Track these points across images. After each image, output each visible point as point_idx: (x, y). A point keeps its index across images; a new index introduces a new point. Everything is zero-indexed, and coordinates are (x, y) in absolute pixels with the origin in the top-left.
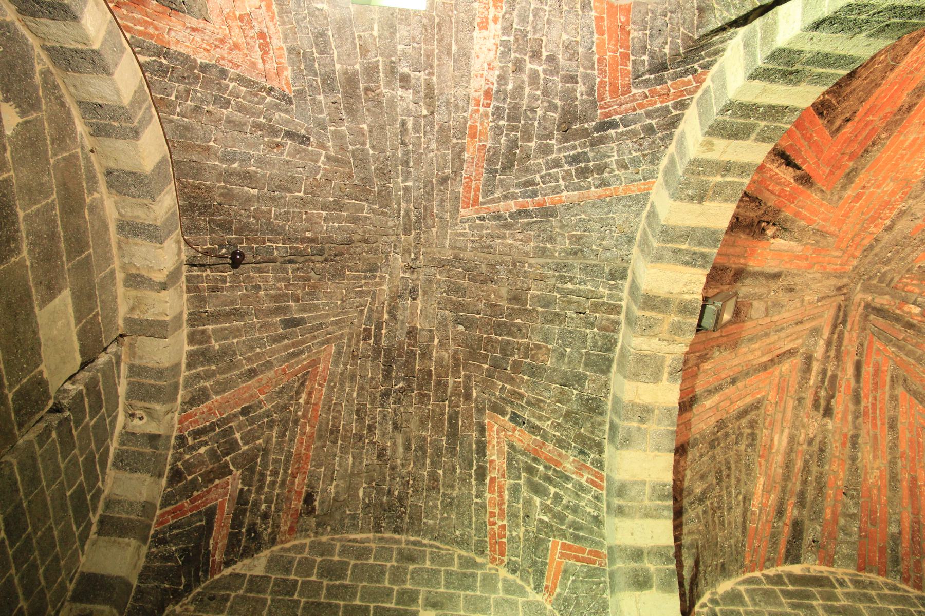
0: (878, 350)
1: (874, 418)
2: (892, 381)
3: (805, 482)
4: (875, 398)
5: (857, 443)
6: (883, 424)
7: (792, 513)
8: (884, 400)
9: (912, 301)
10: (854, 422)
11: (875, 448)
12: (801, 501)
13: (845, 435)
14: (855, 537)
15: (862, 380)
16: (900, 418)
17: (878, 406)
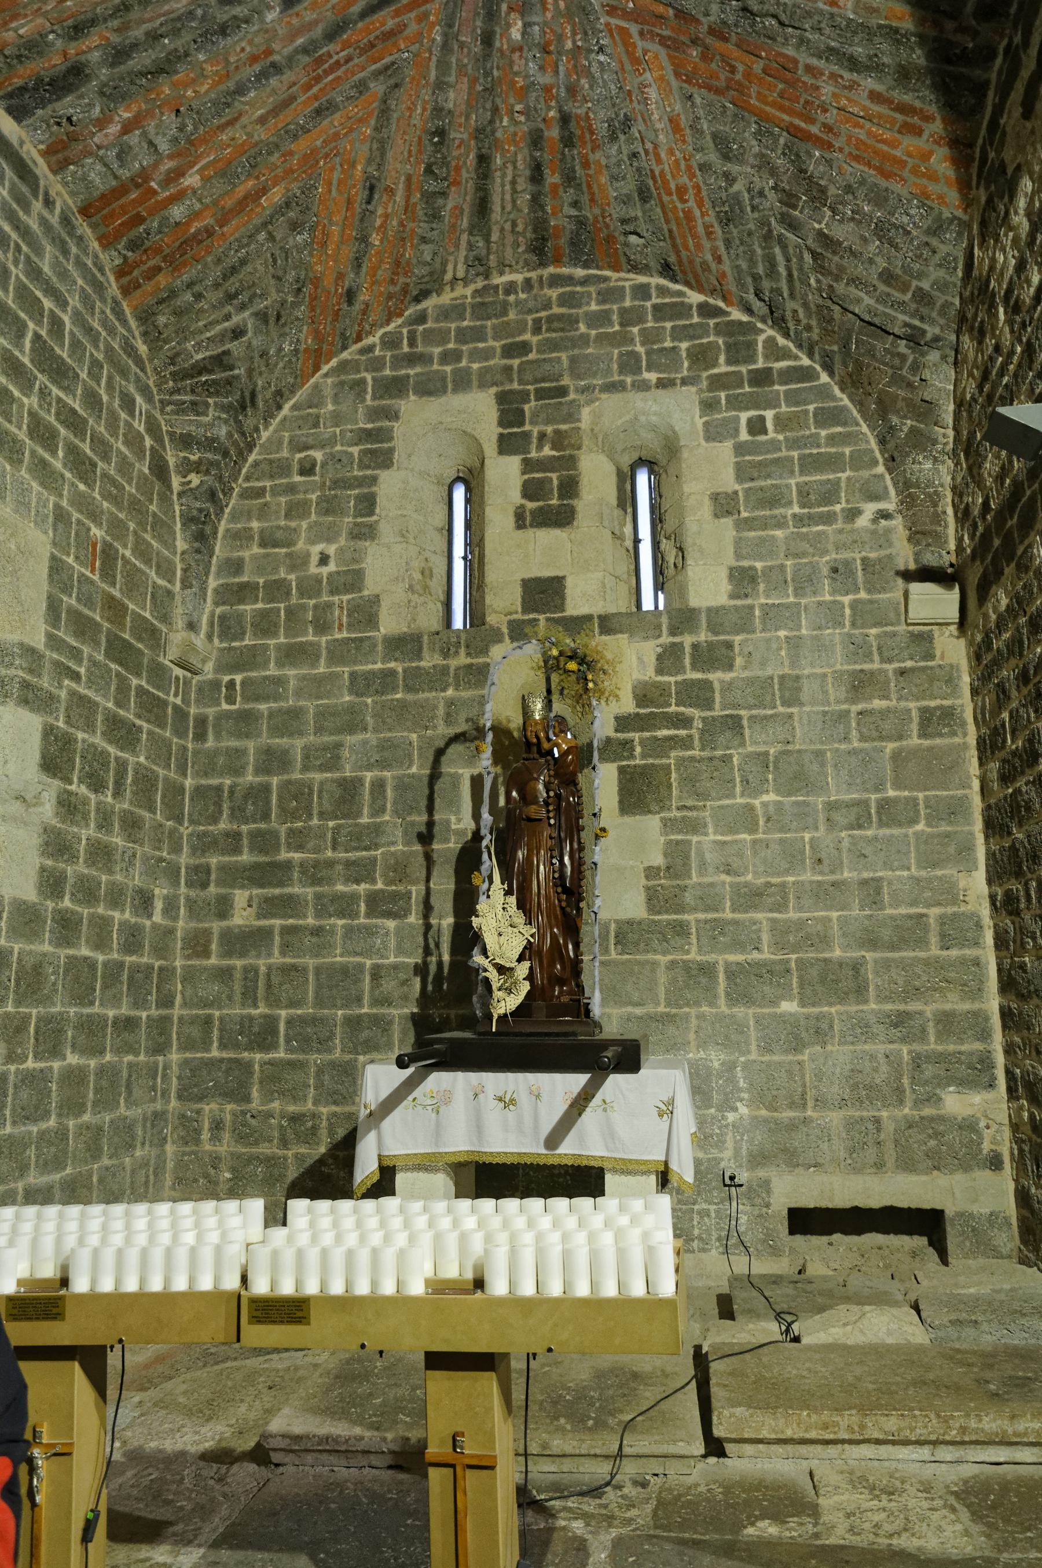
0: (426, 15)
1: (318, 79)
2: (387, 68)
3: (154, 37)
4: (349, 59)
5: (267, 79)
6: (316, 97)
7: (90, 49)
8: (353, 74)
9: (528, 19)
10: (296, 51)
11: (275, 111)
12: (119, 54)
13: (268, 52)
14: (125, 174)
15: (367, 20)
16: (337, 115)
17: (339, 73)
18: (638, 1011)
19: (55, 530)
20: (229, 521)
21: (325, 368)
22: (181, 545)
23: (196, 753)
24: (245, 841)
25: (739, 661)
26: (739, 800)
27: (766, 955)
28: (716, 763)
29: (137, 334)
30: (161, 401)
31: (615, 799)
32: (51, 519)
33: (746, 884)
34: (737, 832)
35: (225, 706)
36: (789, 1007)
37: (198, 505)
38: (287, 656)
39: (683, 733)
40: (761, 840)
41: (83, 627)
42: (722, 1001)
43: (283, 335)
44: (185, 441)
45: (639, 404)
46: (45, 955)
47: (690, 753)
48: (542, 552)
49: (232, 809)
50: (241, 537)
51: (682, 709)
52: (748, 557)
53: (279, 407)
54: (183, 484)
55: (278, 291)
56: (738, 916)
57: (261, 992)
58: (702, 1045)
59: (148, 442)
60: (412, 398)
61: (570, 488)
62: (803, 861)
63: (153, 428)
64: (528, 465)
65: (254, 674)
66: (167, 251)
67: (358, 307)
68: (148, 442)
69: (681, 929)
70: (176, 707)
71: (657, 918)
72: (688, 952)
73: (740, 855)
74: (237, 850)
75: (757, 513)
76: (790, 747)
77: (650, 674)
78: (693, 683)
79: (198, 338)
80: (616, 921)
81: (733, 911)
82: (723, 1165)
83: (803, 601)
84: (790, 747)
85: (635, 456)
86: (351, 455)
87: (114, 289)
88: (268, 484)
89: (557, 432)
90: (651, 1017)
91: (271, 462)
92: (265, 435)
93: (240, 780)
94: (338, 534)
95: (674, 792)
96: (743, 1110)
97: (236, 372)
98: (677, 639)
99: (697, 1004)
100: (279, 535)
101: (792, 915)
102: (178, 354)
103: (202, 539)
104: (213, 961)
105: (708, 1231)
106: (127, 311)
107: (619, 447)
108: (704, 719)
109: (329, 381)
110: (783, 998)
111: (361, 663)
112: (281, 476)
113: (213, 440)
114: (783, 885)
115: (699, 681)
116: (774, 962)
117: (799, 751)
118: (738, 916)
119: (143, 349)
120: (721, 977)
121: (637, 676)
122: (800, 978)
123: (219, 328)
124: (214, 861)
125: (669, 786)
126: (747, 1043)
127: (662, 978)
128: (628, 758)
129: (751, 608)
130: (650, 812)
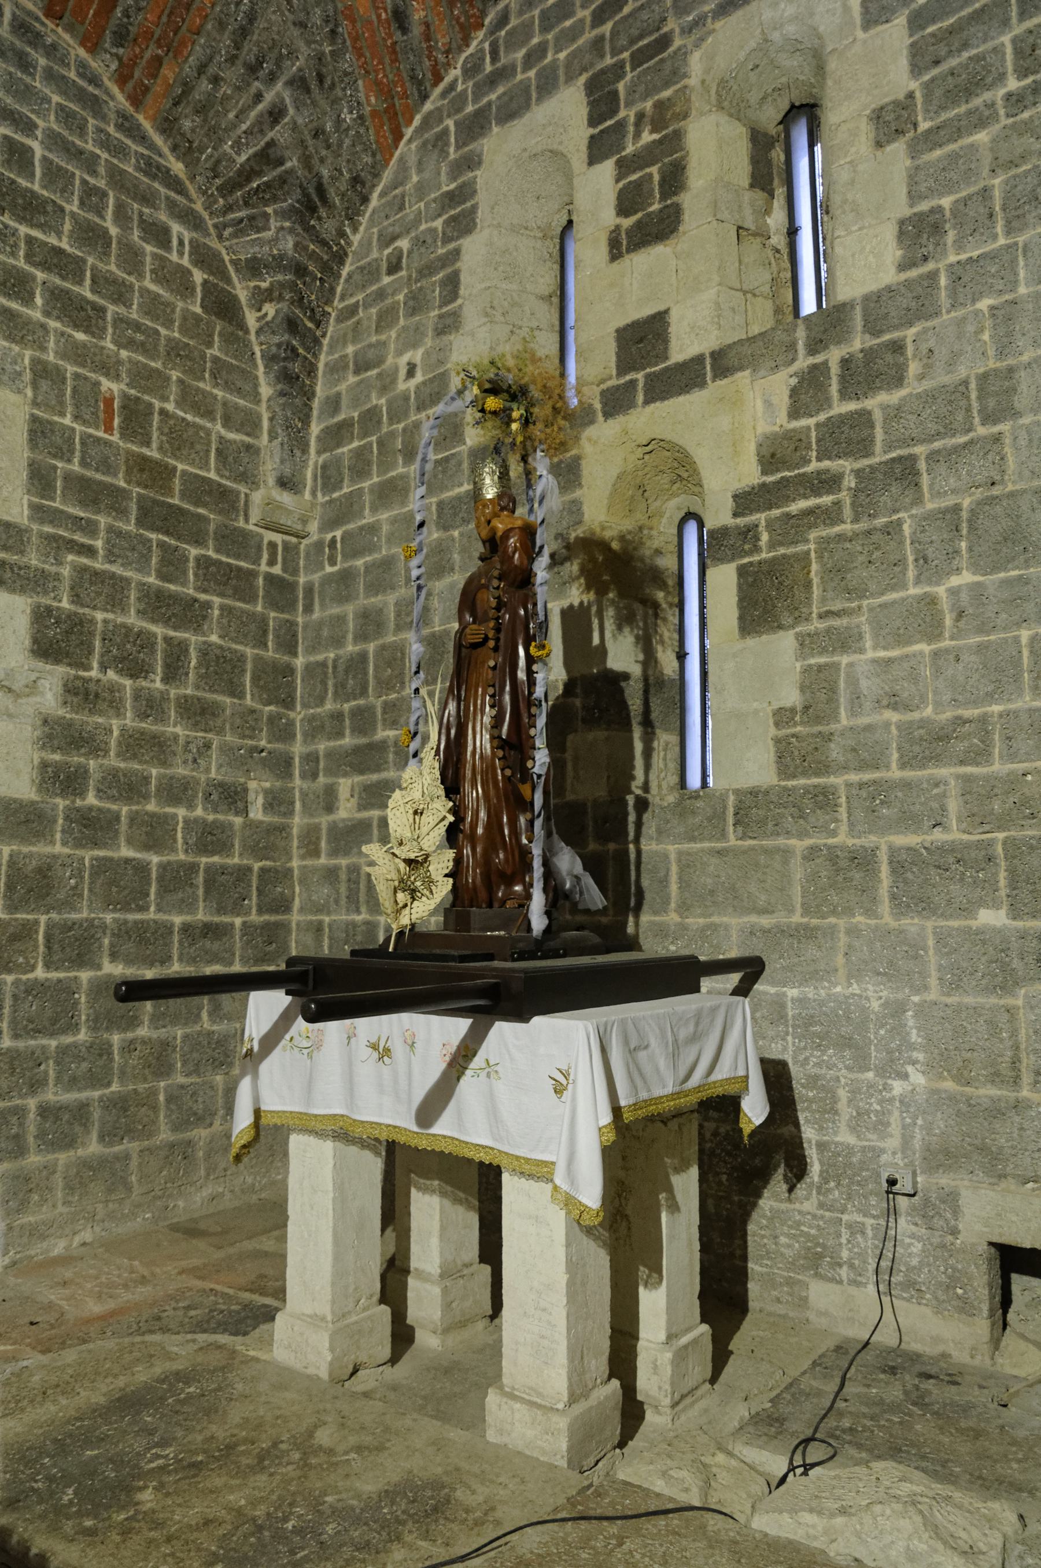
18: (765, 921)
19: (35, 386)
20: (328, 353)
21: (409, 132)
22: (266, 391)
23: (306, 627)
24: (347, 722)
25: (913, 368)
26: (913, 591)
27: (954, 834)
28: (876, 537)
29: (166, 150)
30: (215, 226)
31: (734, 613)
32: (28, 376)
33: (923, 723)
34: (909, 642)
35: (329, 569)
36: (992, 918)
37: (276, 339)
38: (380, 497)
39: (827, 500)
40: (947, 651)
41: (88, 492)
42: (885, 907)
43: (335, 101)
44: (253, 268)
45: (768, 15)
46: (55, 857)
47: (837, 529)
48: (645, 283)
49: (335, 686)
50: (337, 369)
51: (826, 464)
52: (932, 192)
53: (365, 200)
54: (259, 319)
55: (308, 43)
56: (909, 774)
57: (362, 896)
58: (855, 974)
59: (198, 276)
60: (496, 129)
61: (674, 179)
62: (1017, 679)
63: (204, 258)
64: (624, 167)
65: (351, 526)
66: (158, 32)
67: (417, 31)
68: (198, 276)
69: (824, 799)
70: (270, 578)
71: (790, 783)
72: (834, 833)
73: (914, 677)
74: (340, 734)
75: (944, 116)
76: (996, 491)
77: (782, 421)
78: (843, 419)
79: (234, 135)
80: (737, 792)
81: (903, 766)
82: (884, 1158)
83: (1021, 240)
84: (996, 491)
85: (785, 106)
86: (435, 230)
87: (121, 99)
88: (360, 297)
89: (659, 105)
90: (781, 931)
91: (362, 269)
92: (356, 239)
93: (341, 652)
94: (424, 335)
95: (816, 592)
96: (917, 1078)
97: (289, 165)
98: (819, 359)
99: (849, 911)
100: (371, 354)
101: (998, 767)
102: (218, 162)
103: (295, 381)
104: (323, 860)
105: (862, 1255)
106: (147, 125)
107: (754, 97)
108: (858, 473)
109: (413, 146)
110: (982, 903)
111: (447, 489)
112: (371, 284)
113: (282, 257)
114: (983, 720)
115: (852, 414)
116: (968, 846)
117: (1012, 495)
118: (909, 774)
119: (178, 167)
120: (885, 870)
121: (764, 427)
122: (1012, 872)
123: (253, 114)
124: (322, 746)
125: (808, 585)
126: (924, 975)
127: (798, 872)
128: (750, 553)
129: (933, 276)
130: (780, 627)
